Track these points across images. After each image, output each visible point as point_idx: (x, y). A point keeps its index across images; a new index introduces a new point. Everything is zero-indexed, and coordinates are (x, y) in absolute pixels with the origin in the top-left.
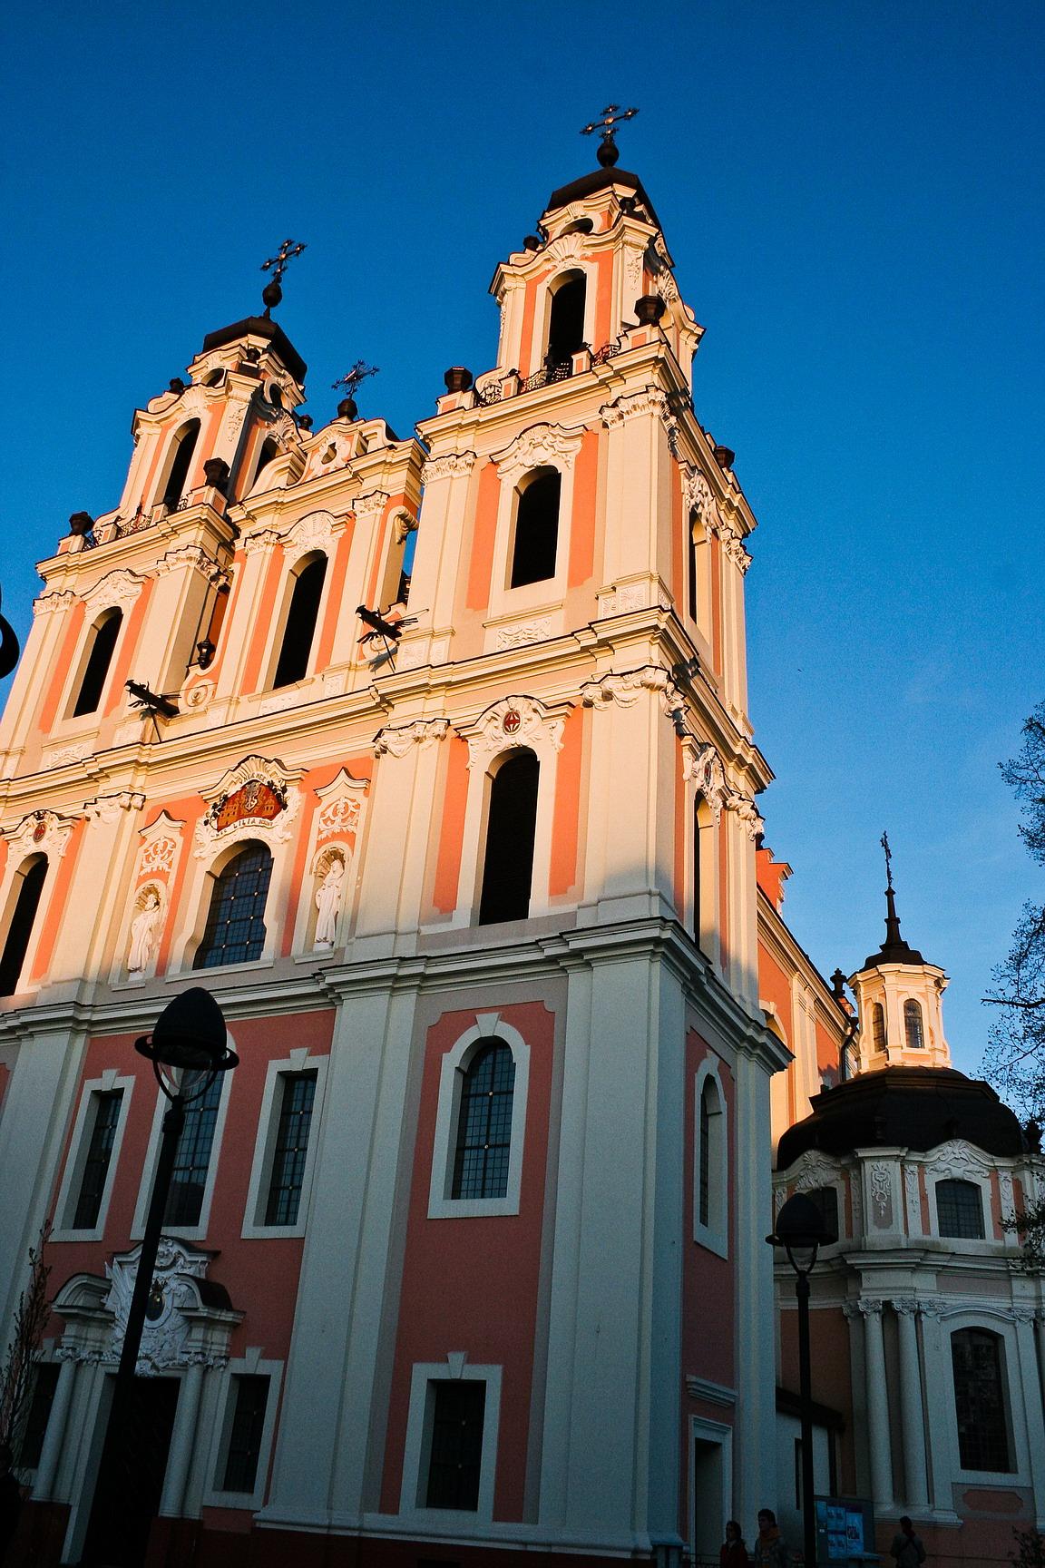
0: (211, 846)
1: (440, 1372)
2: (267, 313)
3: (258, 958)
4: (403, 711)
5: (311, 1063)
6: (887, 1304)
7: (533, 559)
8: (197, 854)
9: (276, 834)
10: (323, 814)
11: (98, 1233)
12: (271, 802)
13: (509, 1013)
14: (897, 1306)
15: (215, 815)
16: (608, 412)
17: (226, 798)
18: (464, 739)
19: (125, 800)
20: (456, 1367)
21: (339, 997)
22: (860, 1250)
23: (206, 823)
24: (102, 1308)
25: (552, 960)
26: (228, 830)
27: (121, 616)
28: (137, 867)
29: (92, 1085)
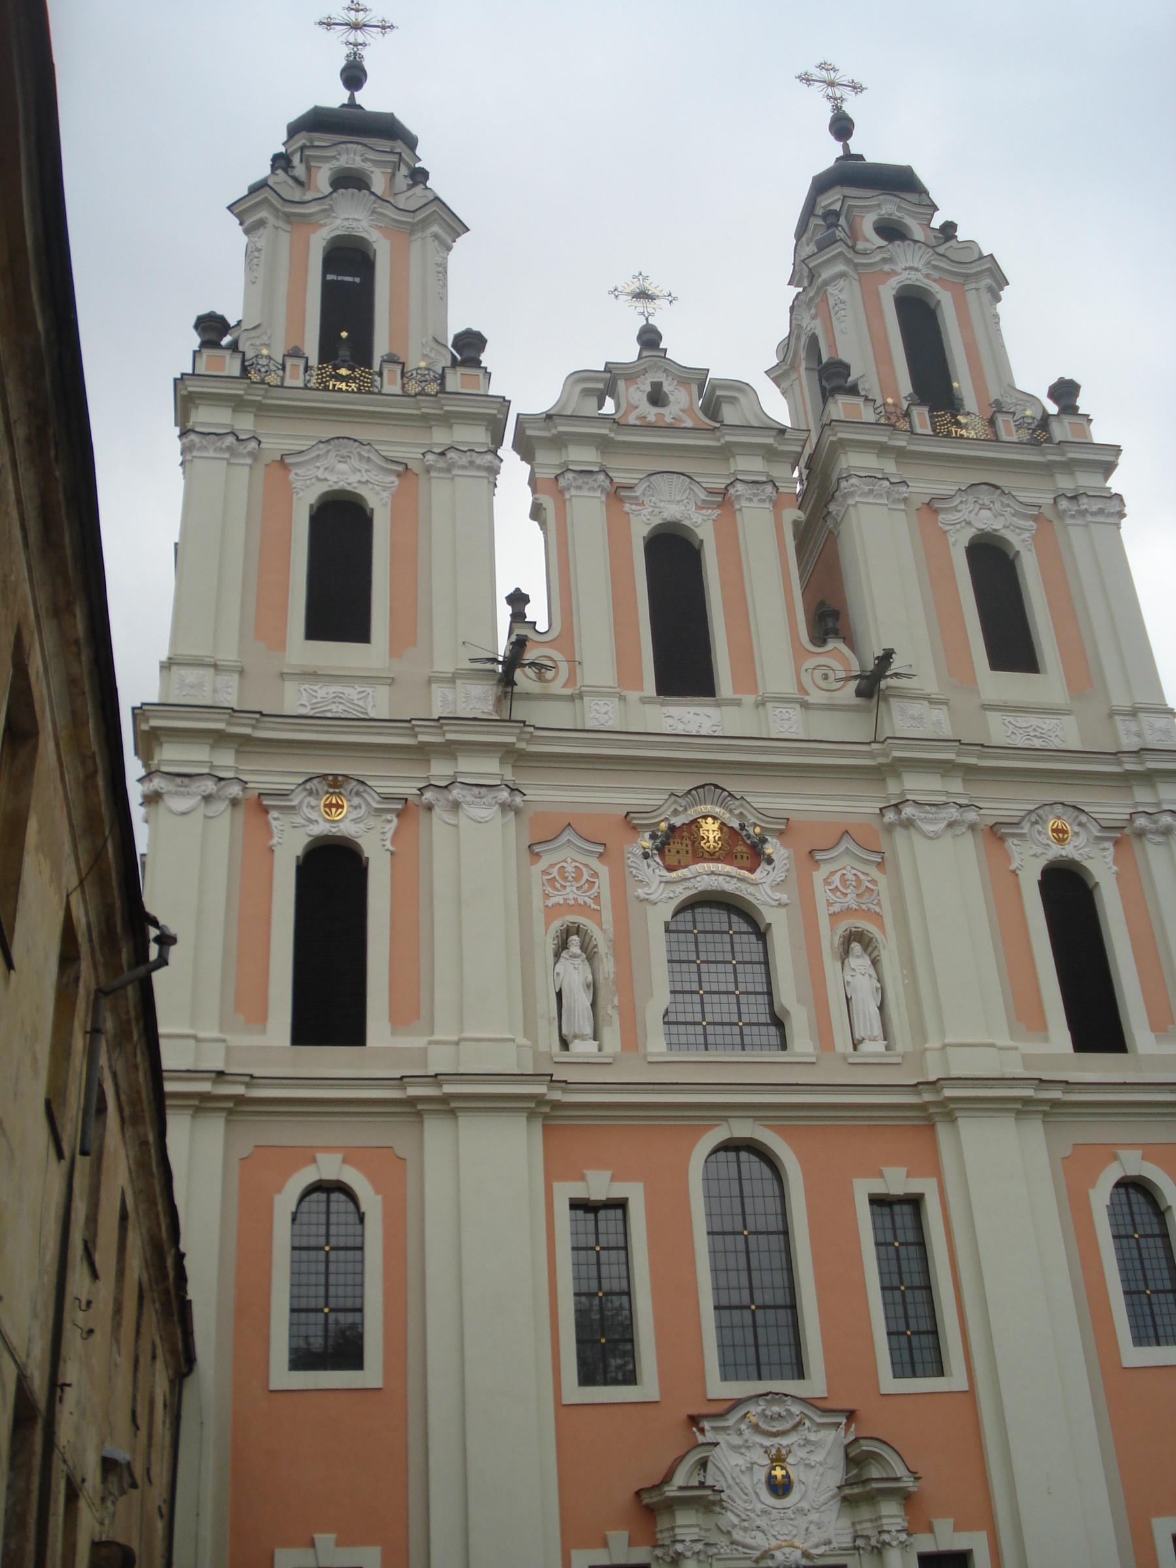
0: (661, 889)
8: (641, 892)
9: (763, 888)
10: (826, 882)
11: (648, 1387)
12: (740, 848)
13: (1150, 1152)
16: (1064, 504)
17: (672, 828)
18: (1002, 839)
23: (646, 856)
28: (537, 892)
29: (566, 1190)
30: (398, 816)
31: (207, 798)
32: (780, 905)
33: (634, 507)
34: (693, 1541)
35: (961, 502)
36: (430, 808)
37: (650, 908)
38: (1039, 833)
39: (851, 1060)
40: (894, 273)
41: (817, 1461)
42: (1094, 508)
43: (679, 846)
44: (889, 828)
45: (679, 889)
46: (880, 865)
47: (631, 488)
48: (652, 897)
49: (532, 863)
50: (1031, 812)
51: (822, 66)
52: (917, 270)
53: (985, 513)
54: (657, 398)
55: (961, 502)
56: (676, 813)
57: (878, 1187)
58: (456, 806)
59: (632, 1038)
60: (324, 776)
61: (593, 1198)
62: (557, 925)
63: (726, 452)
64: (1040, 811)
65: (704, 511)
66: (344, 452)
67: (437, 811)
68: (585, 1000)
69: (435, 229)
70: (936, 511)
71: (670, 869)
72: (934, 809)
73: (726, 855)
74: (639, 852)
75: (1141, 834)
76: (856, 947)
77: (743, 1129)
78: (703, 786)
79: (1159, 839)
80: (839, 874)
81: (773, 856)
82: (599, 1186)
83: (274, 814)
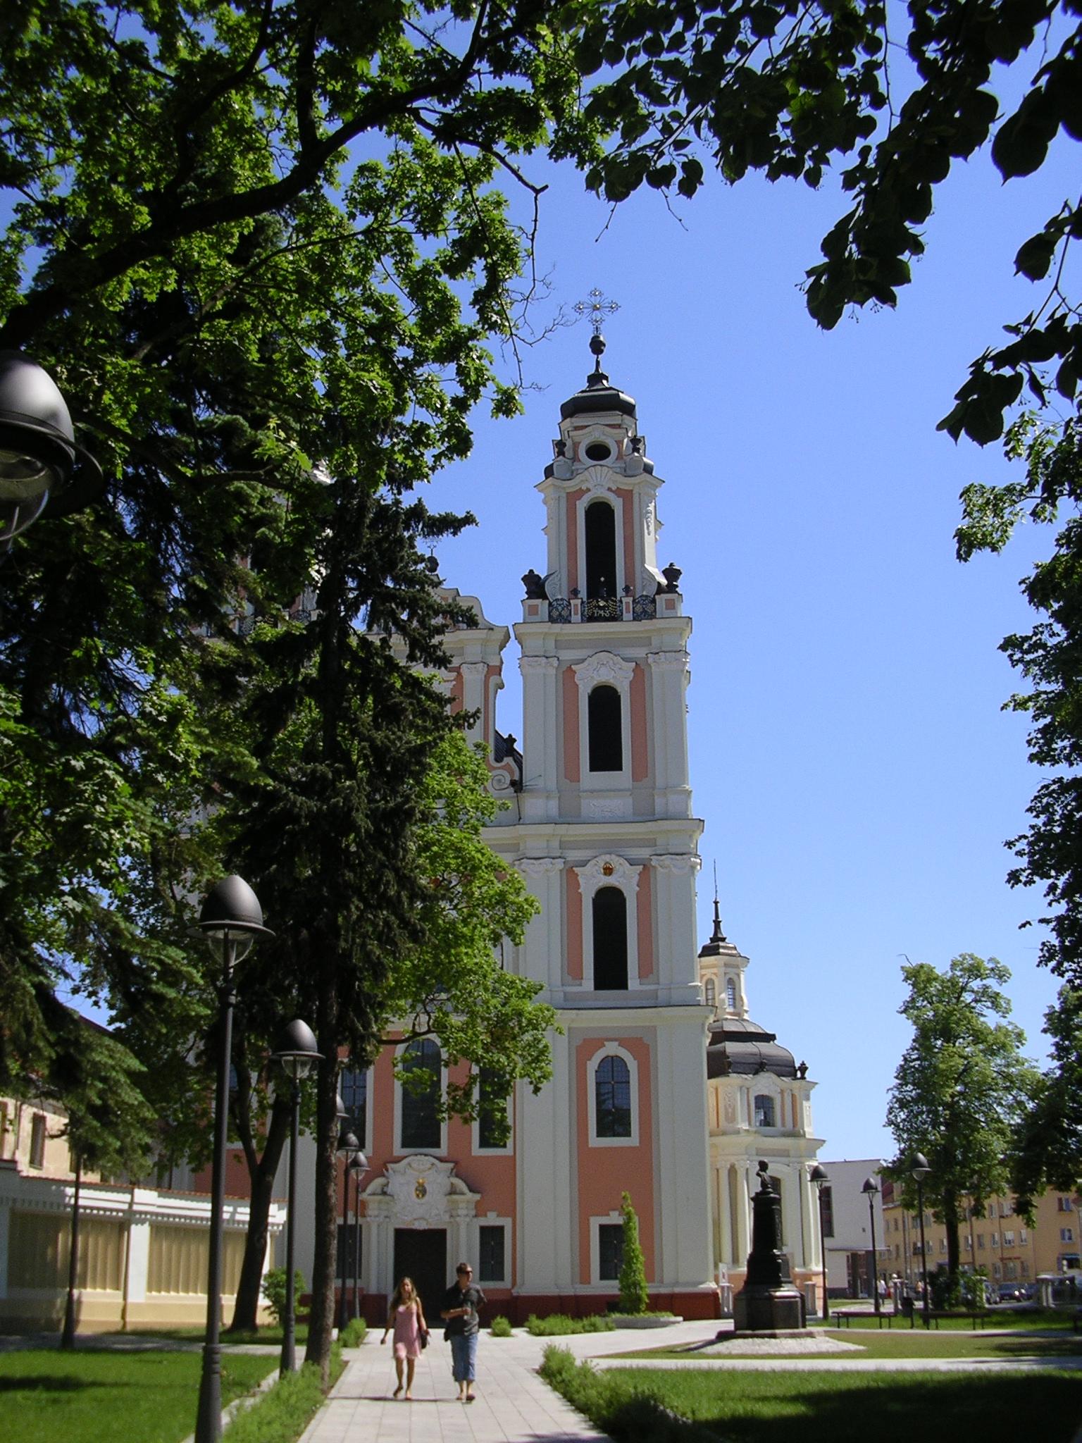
7: (605, 754)
16: (651, 658)
20: (615, 1219)
24: (384, 1193)
40: (588, 490)
53: (603, 670)
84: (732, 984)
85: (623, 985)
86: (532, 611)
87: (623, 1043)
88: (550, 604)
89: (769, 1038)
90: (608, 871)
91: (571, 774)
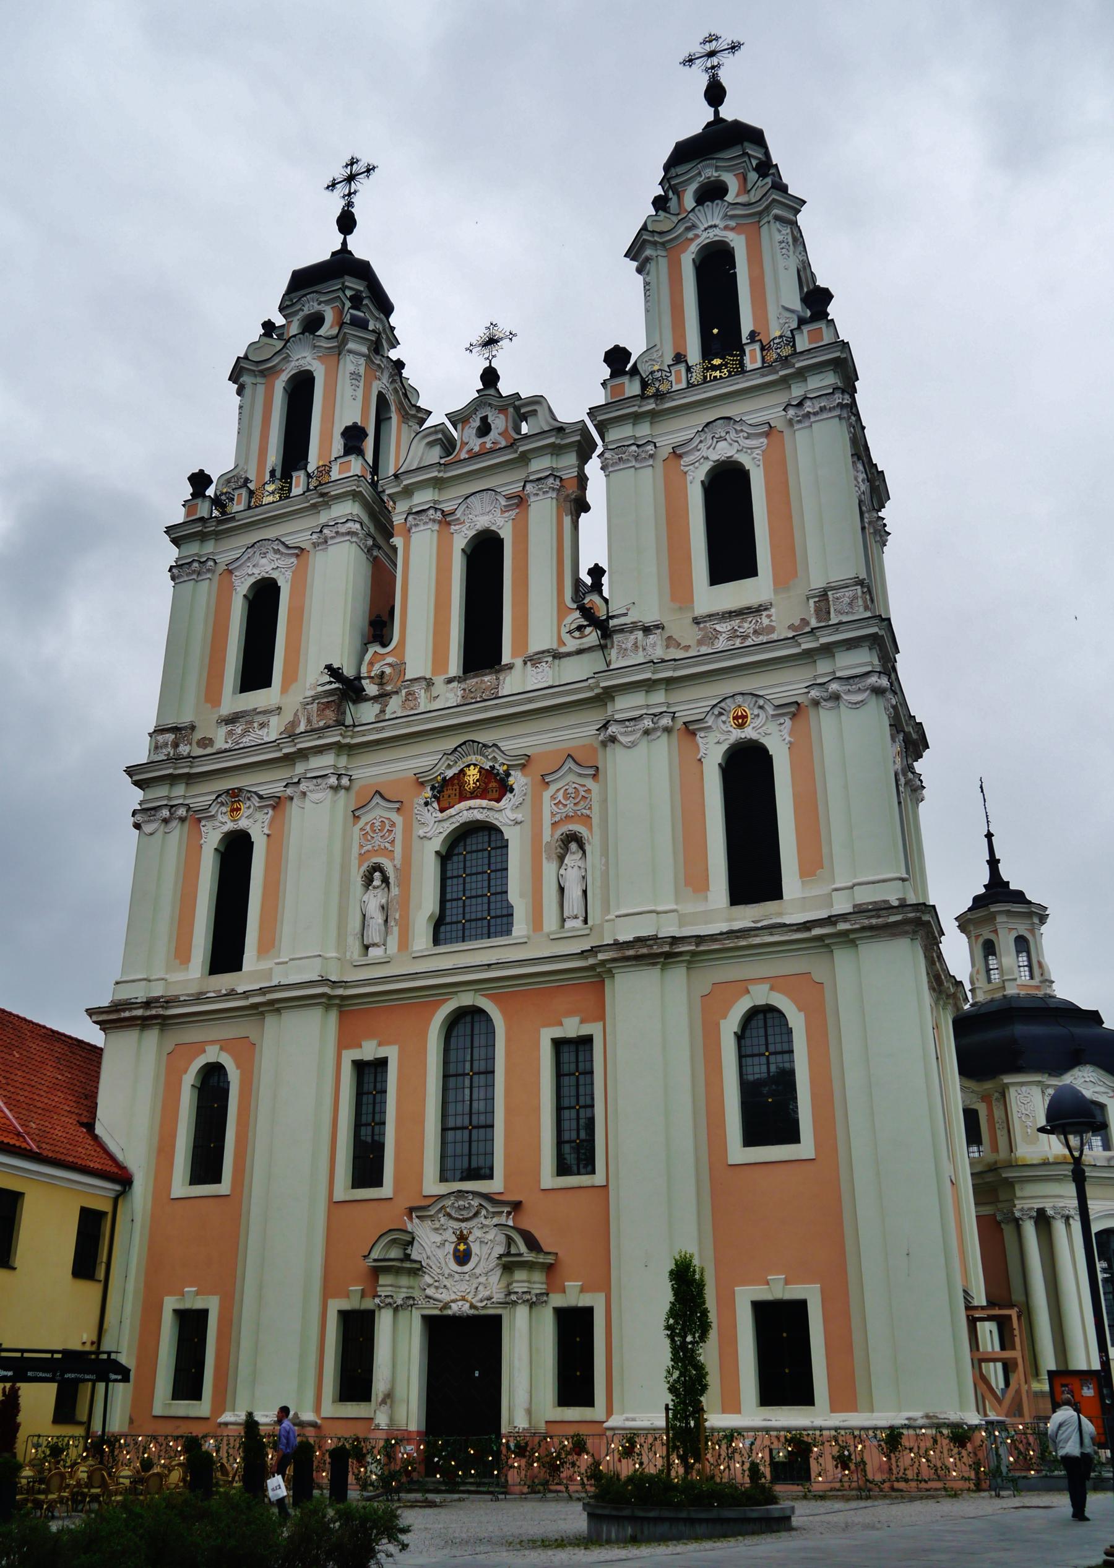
0: (434, 828)
1: (764, 1293)
2: (344, 243)
3: (509, 932)
4: (625, 705)
5: (585, 1030)
6: (1041, 1212)
8: (421, 833)
9: (505, 814)
10: (553, 798)
12: (493, 784)
14: (1050, 1212)
15: (434, 796)
17: (444, 779)
18: (693, 733)
19: (333, 780)
20: (778, 1290)
21: (610, 971)
22: (1011, 1165)
23: (426, 804)
25: (820, 938)
26: (452, 811)
27: (277, 589)
29: (350, 1055)
30: (274, 808)
31: (166, 821)
32: (517, 823)
33: (457, 527)
34: (524, 1293)
35: (701, 442)
36: (291, 798)
37: (426, 842)
38: (724, 722)
39: (552, 937)
41: (488, 1244)
42: (817, 409)
43: (450, 792)
44: (604, 744)
45: (446, 824)
46: (595, 776)
47: (453, 513)
48: (428, 835)
49: (354, 824)
50: (714, 706)
51: (704, 42)
52: (715, 226)
53: (722, 444)
54: (484, 429)
55: (701, 442)
56: (449, 767)
57: (558, 1033)
58: (304, 794)
59: (404, 943)
60: (227, 792)
61: (366, 1059)
62: (364, 868)
63: (524, 459)
64: (722, 705)
65: (506, 514)
66: (264, 550)
67: (295, 799)
68: (380, 920)
69: (351, 345)
70: (680, 456)
71: (442, 811)
72: (632, 723)
73: (480, 792)
74: (422, 802)
75: (816, 703)
76: (573, 846)
77: (466, 999)
78: (464, 743)
79: (829, 704)
80: (562, 791)
81: (514, 786)
82: (369, 1051)
83: (203, 823)
84: (1022, 944)
85: (774, 892)
86: (615, 391)
87: (775, 983)
88: (644, 385)
89: (1094, 1017)
90: (741, 721)
91: (679, 589)
